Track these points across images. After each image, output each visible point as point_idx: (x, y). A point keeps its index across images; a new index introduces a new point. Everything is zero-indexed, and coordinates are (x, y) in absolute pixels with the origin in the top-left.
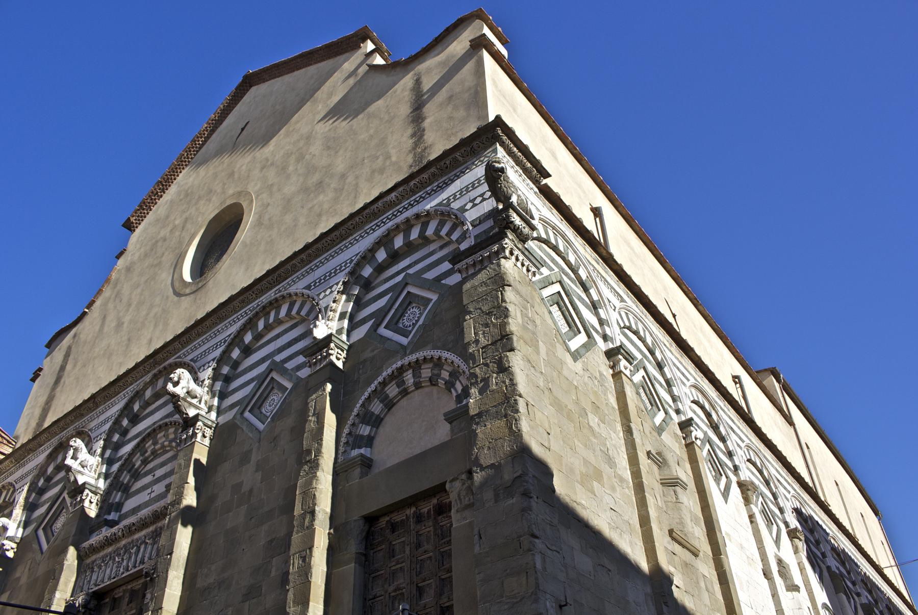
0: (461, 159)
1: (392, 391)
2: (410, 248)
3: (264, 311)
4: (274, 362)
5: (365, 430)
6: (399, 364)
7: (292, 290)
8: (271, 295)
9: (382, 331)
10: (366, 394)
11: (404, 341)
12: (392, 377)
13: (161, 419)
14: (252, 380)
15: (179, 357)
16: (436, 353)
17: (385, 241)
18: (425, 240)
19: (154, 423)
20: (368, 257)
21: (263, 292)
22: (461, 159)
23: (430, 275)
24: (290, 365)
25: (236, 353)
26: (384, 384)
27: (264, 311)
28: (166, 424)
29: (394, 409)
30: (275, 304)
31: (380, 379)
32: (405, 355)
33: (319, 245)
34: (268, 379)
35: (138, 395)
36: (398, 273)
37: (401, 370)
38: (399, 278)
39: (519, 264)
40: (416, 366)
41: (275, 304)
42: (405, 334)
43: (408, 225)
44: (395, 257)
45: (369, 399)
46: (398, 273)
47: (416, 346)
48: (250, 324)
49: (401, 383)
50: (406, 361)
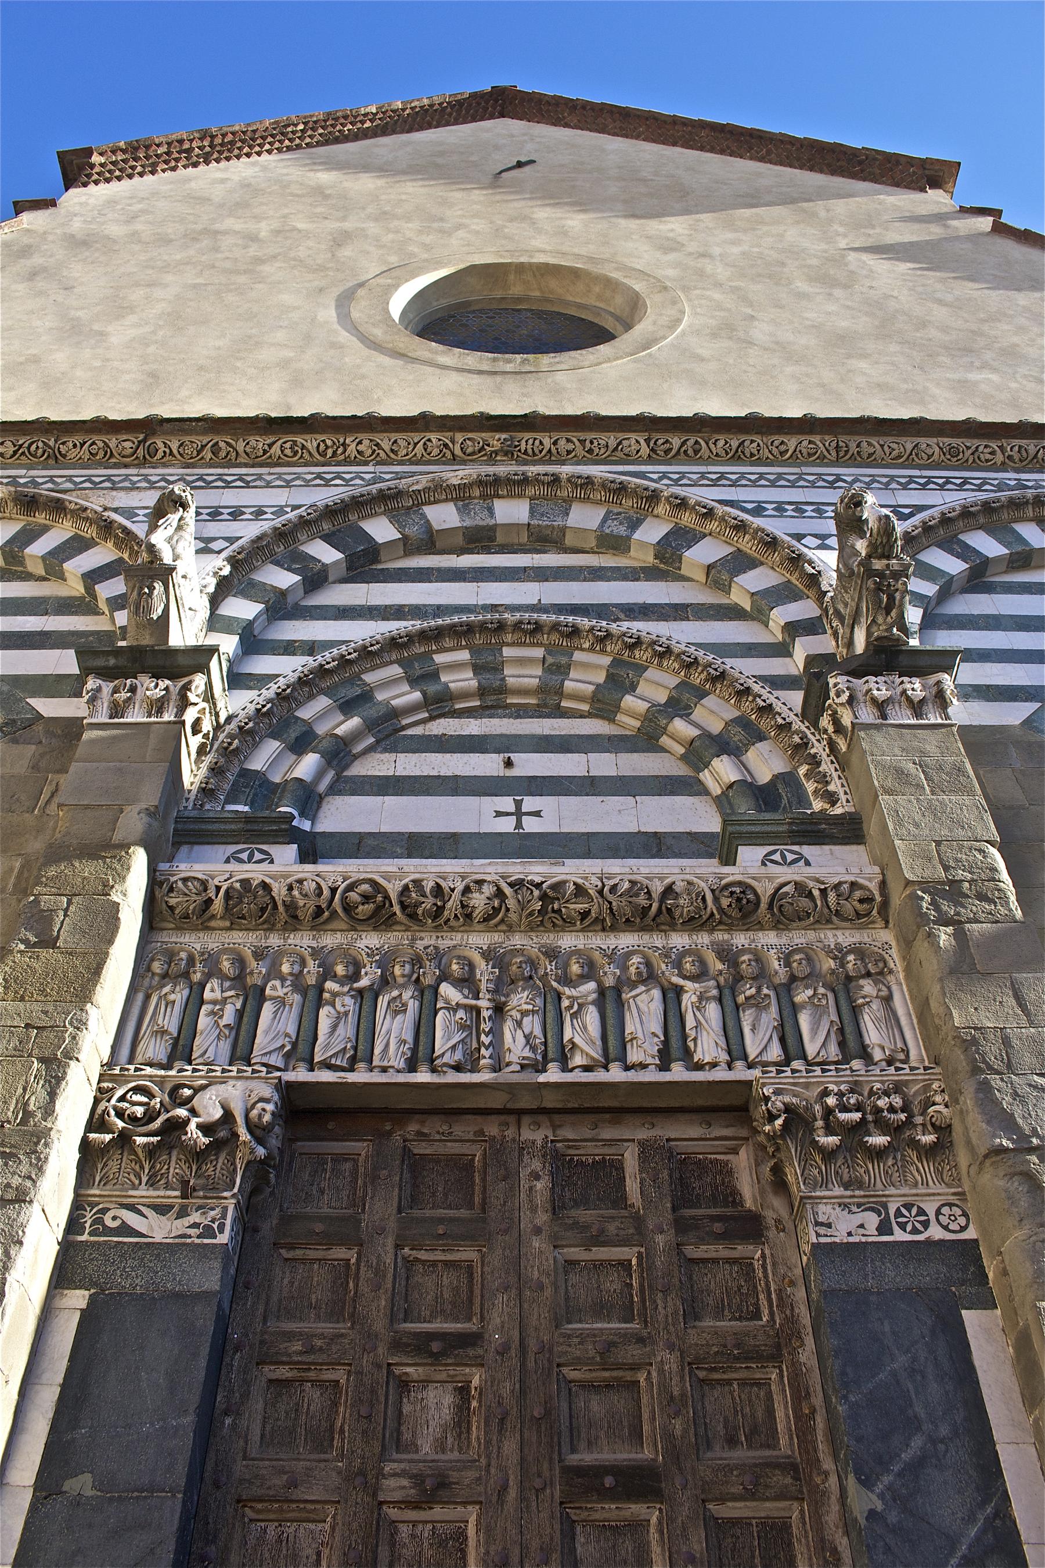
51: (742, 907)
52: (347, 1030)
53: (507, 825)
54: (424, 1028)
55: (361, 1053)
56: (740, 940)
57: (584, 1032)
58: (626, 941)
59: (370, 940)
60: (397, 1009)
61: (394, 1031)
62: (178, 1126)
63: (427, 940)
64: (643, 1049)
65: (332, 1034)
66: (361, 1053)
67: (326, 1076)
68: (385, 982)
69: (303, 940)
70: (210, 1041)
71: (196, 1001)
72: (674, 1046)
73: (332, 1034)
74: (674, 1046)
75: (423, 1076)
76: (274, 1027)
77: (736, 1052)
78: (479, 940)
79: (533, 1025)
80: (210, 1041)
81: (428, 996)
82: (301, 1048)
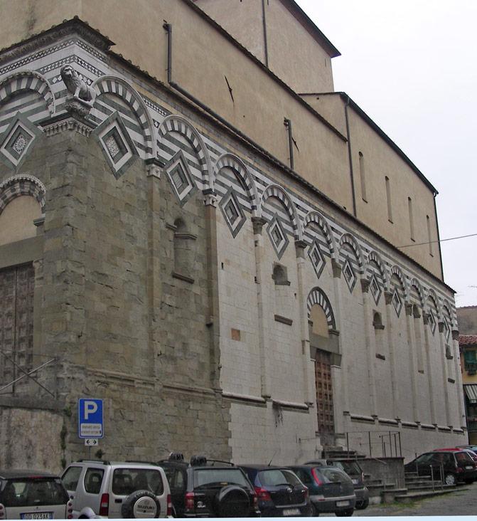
0: (53, 38)
2: (21, 93)
6: (12, 179)
11: (16, 162)
12: (8, 185)
18: (28, 91)
22: (53, 38)
29: (9, 204)
32: (15, 173)
36: (14, 109)
37: (13, 182)
38: (14, 114)
39: (80, 131)
40: (22, 181)
42: (16, 157)
43: (19, 78)
46: (14, 109)
47: (23, 168)
49: (13, 190)
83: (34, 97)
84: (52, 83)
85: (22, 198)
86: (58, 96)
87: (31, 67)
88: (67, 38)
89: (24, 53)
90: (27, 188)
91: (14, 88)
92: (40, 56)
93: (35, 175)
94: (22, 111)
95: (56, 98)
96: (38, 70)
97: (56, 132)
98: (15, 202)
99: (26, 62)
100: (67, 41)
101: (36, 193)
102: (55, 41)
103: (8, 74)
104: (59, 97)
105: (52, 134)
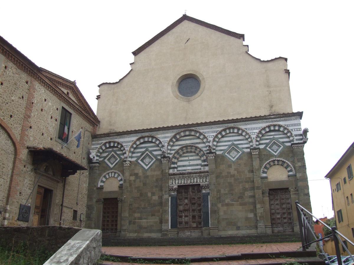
1: (272, 164)
3: (229, 128)
4: (233, 143)
5: (266, 170)
6: (275, 159)
7: (240, 127)
8: (232, 125)
9: (268, 148)
10: (266, 163)
11: (276, 154)
12: (272, 161)
13: (190, 144)
14: (226, 145)
15: (196, 129)
16: (285, 160)
17: (269, 127)
19: (187, 144)
20: (264, 129)
21: (230, 123)
23: (281, 140)
24: (240, 146)
25: (220, 136)
26: (270, 162)
27: (229, 128)
28: (193, 146)
30: (233, 128)
31: (270, 161)
32: (276, 157)
33: (249, 119)
34: (232, 147)
35: (179, 133)
37: (274, 160)
38: (272, 137)
40: (278, 161)
41: (233, 128)
42: (276, 152)
43: (275, 126)
44: (270, 131)
45: (266, 164)
48: (224, 130)
50: (277, 159)
51: (201, 172)
52: (180, 182)
53: (188, 164)
54: (184, 181)
55: (181, 183)
56: (201, 174)
57: (192, 181)
58: (195, 175)
59: (181, 176)
60: (183, 180)
61: (183, 181)
62: (173, 189)
63: (184, 175)
64: (195, 182)
65: (180, 182)
66: (181, 183)
67: (180, 185)
68: (182, 178)
69: (177, 176)
70: (174, 183)
71: (172, 181)
72: (197, 182)
73: (180, 182)
74: (197, 182)
75: (184, 184)
76: (177, 182)
77: (200, 182)
78: (187, 175)
79: (190, 181)
80: (174, 183)
81: (184, 179)
82: (178, 183)
83: (280, 133)
84: (293, 131)
85: (277, 166)
86: (296, 136)
87: (281, 123)
88: (296, 117)
89: (282, 117)
90: (280, 163)
91: (272, 128)
92: (285, 120)
93: (286, 160)
94: (275, 137)
95: (295, 136)
96: (285, 125)
97: (297, 148)
98: (274, 167)
99: (279, 121)
100: (297, 118)
101: (285, 165)
102: (291, 117)
103: (271, 123)
104: (296, 136)
105: (296, 148)
